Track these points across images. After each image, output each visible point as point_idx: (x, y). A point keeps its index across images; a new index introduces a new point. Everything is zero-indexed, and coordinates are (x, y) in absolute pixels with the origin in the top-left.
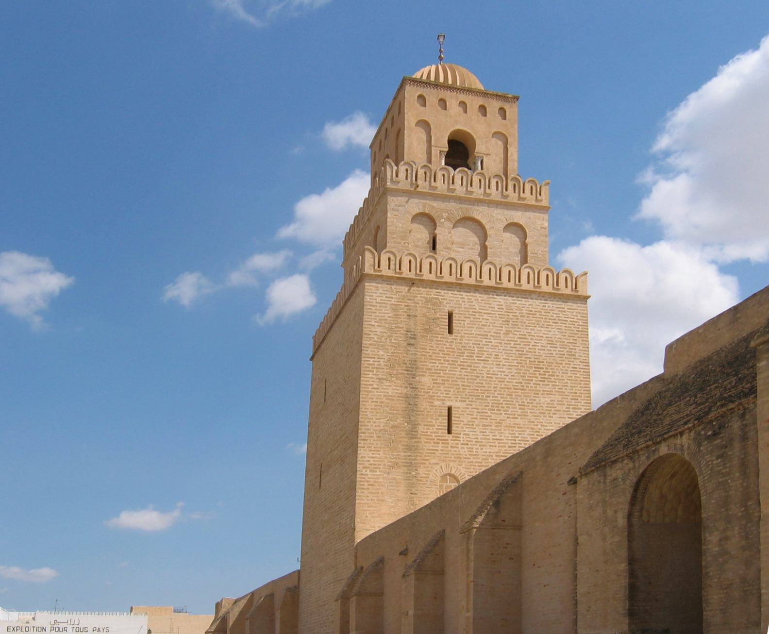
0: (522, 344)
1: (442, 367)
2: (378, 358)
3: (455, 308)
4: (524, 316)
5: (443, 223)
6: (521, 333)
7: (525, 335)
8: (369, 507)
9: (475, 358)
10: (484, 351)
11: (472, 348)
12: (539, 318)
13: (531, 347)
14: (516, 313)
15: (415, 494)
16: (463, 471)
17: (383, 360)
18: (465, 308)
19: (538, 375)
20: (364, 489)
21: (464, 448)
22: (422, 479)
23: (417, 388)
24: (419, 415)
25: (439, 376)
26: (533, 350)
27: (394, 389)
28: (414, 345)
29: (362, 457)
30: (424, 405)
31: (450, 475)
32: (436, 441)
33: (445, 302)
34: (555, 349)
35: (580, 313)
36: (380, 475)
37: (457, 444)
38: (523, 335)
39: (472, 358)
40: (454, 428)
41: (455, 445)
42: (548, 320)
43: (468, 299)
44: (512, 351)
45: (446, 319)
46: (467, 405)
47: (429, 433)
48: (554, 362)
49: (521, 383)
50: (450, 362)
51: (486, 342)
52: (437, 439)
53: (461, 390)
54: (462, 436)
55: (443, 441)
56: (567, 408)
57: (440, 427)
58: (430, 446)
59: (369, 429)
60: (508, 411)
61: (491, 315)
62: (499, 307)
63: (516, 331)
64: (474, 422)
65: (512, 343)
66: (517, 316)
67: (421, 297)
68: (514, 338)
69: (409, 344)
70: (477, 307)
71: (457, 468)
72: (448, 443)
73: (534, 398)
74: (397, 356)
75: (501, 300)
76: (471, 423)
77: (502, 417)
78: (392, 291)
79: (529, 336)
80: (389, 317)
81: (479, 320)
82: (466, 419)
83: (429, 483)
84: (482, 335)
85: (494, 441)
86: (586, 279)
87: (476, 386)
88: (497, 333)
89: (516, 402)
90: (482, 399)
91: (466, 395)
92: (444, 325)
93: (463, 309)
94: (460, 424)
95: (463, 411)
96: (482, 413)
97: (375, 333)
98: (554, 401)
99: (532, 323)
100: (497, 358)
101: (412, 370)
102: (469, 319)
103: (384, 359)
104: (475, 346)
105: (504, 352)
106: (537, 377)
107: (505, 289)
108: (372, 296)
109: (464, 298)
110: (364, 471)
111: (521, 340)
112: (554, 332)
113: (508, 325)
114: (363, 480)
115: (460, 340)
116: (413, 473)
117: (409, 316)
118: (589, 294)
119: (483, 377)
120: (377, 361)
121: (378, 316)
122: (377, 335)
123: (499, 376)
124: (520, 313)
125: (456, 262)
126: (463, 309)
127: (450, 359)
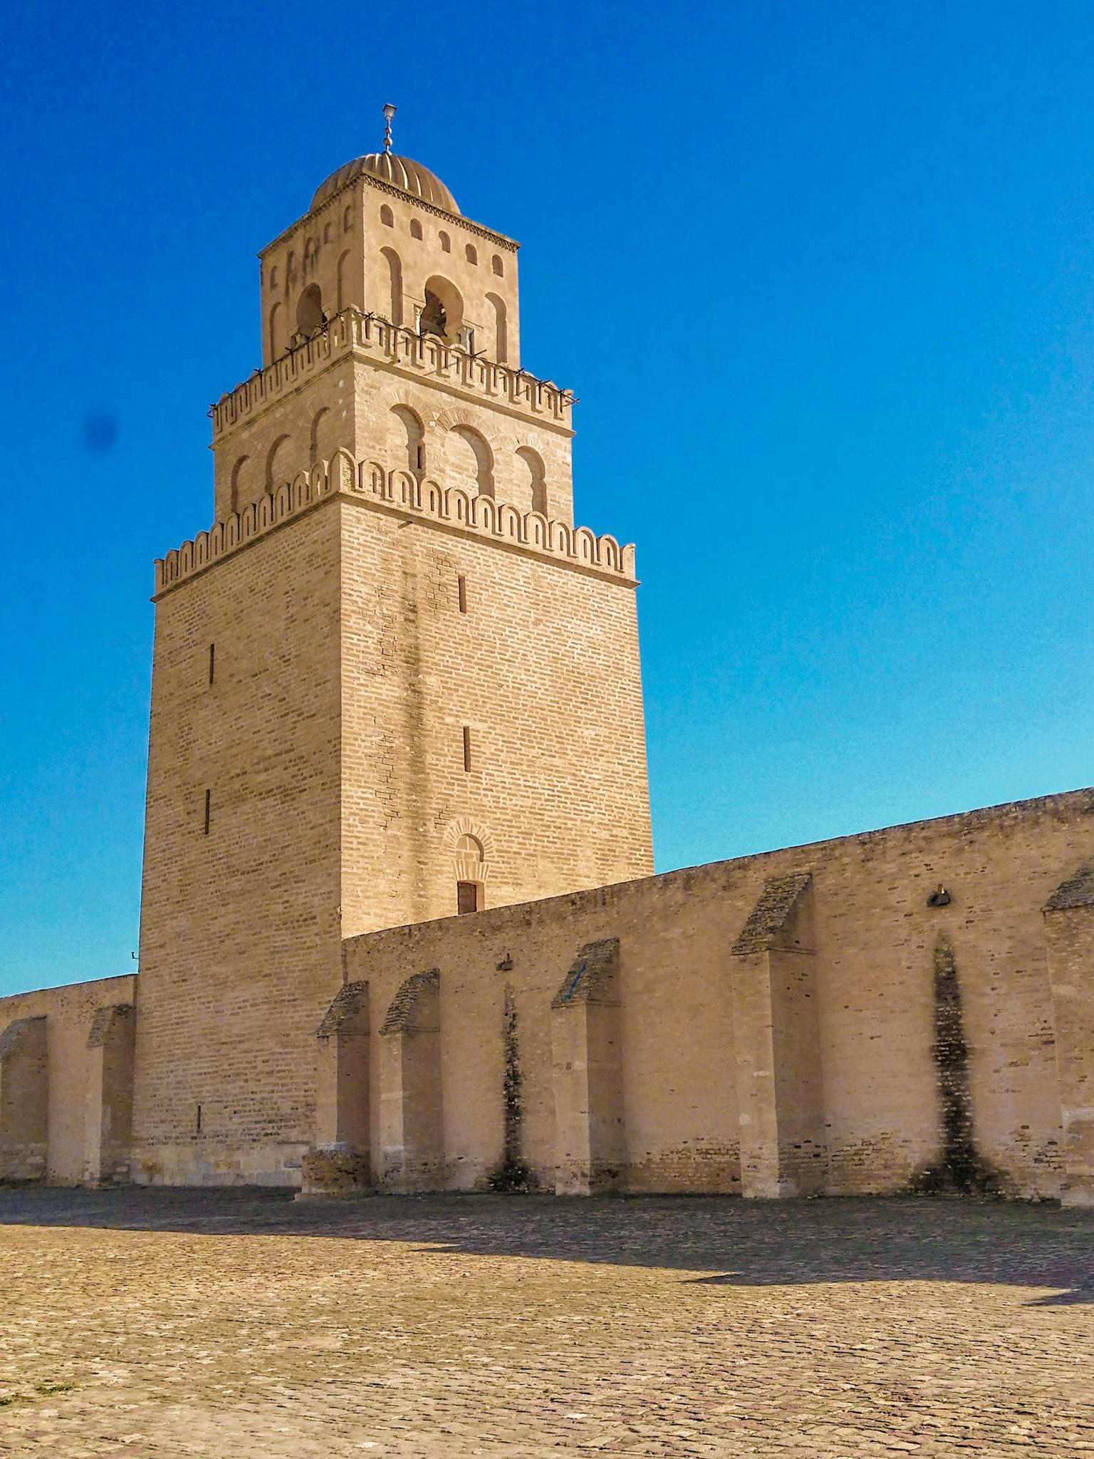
8: (361, 880)
15: (425, 863)
16: (488, 832)
21: (486, 795)
23: (420, 692)
27: (390, 689)
29: (348, 797)
30: (430, 719)
31: (470, 836)
37: (478, 788)
54: (483, 776)
70: (496, 574)
75: (528, 565)
101: (414, 661)
117: (405, 573)
125: (466, 498)
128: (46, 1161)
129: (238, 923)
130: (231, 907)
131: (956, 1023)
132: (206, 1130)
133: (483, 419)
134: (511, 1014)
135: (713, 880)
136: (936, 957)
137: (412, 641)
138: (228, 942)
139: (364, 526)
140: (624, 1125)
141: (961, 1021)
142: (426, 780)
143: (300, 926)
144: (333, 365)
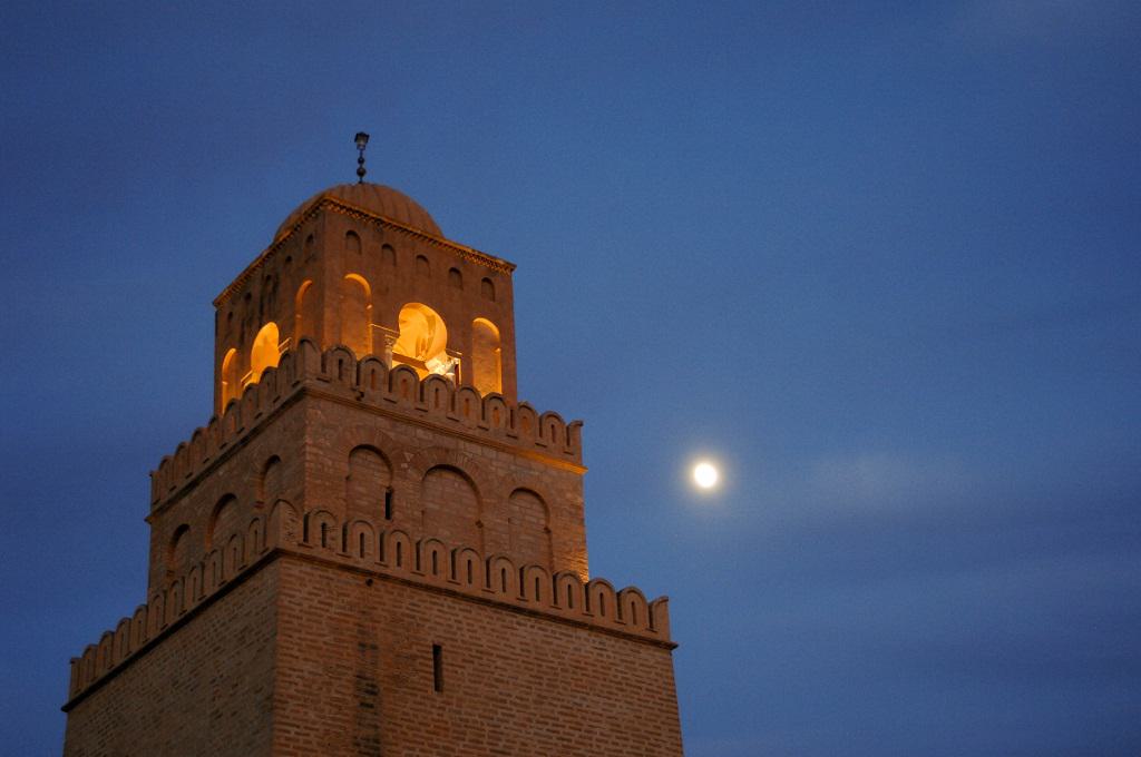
0: (568, 725)
2: (306, 728)
3: (446, 639)
4: (566, 671)
5: (405, 470)
6: (565, 703)
9: (485, 746)
10: (502, 733)
11: (479, 726)
12: (594, 677)
13: (583, 733)
14: (552, 662)
17: (315, 732)
18: (463, 641)
26: (586, 741)
28: (372, 706)
33: (428, 625)
34: (625, 742)
38: (567, 708)
39: (480, 745)
42: (607, 683)
43: (468, 624)
44: (551, 738)
51: (503, 714)
61: (510, 662)
62: (524, 647)
63: (554, 699)
65: (550, 721)
67: (383, 610)
68: (553, 711)
69: (362, 704)
70: (483, 642)
74: (341, 727)
75: (527, 630)
78: (331, 592)
80: (325, 643)
81: (487, 669)
84: (496, 700)
86: (666, 610)
88: (522, 699)
92: (427, 672)
93: (459, 643)
97: (300, 674)
99: (582, 687)
100: (525, 751)
102: (471, 665)
103: (317, 730)
105: (536, 738)
107: (533, 613)
109: (460, 622)
111: (567, 718)
112: (621, 707)
113: (540, 684)
117: (361, 645)
118: (673, 640)
120: (304, 735)
121: (305, 639)
122: (302, 678)
124: (559, 663)
126: (459, 643)
127: (441, 744)
133: (467, 454)
137: (371, 732)
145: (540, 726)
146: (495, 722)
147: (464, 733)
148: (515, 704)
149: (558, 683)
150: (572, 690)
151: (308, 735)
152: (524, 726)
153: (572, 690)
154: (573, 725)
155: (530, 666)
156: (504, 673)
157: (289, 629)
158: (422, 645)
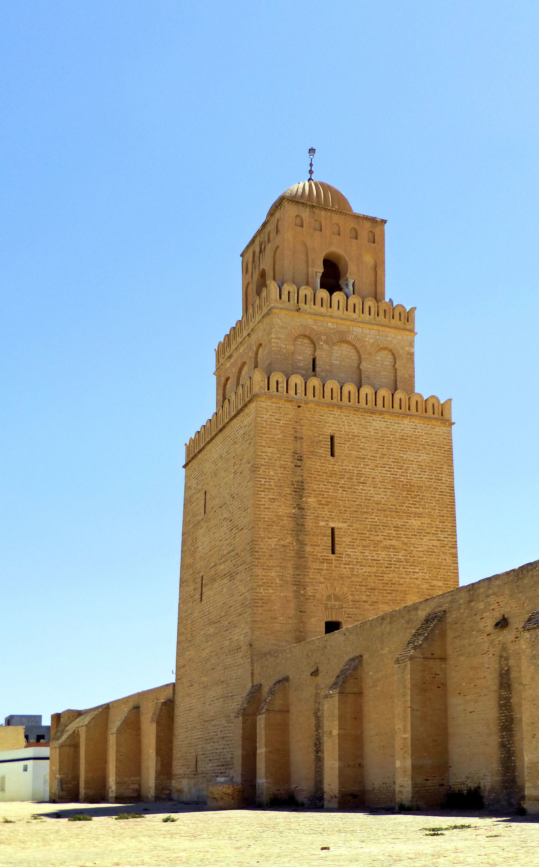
0: (396, 467)
1: (325, 488)
6: (394, 457)
7: (398, 459)
10: (363, 474)
19: (410, 499)
20: (258, 607)
21: (346, 568)
22: (310, 597)
24: (306, 535)
25: (323, 498)
26: (405, 474)
30: (309, 523)
32: (321, 560)
34: (424, 473)
35: (445, 439)
36: (273, 593)
38: (396, 459)
40: (337, 548)
41: (338, 565)
42: (417, 445)
44: (387, 474)
45: (328, 442)
46: (349, 526)
47: (315, 553)
48: (423, 485)
49: (395, 505)
50: (333, 484)
52: (323, 559)
53: (343, 511)
55: (328, 561)
56: (435, 531)
57: (325, 547)
58: (317, 565)
59: (261, 548)
60: (384, 532)
63: (390, 455)
64: (354, 542)
66: (391, 440)
71: (341, 587)
72: (332, 563)
73: (407, 521)
76: (352, 544)
77: (378, 538)
79: (402, 460)
82: (347, 540)
83: (316, 601)
85: (372, 561)
87: (356, 508)
89: (391, 524)
90: (361, 521)
91: (347, 516)
94: (342, 544)
95: (345, 532)
96: (362, 534)
98: (425, 523)
104: (355, 469)
106: (409, 500)
108: (263, 418)
110: (258, 589)
111: (396, 464)
112: (424, 456)
114: (257, 598)
115: (341, 463)
116: (302, 592)
119: (362, 499)
123: (376, 499)
128: (140, 785)
129: (212, 652)
130: (209, 643)
131: (509, 702)
132: (199, 770)
134: (318, 702)
135: (403, 617)
136: (500, 661)
138: (208, 663)
139: (269, 413)
140: (363, 767)
141: (512, 701)
142: (306, 561)
143: (235, 653)
144: (263, 317)
145: (382, 469)
146: (360, 469)
147: (345, 475)
148: (370, 459)
149: (392, 448)
150: (399, 450)
151: (270, 482)
152: (374, 470)
153: (399, 450)
154: (399, 467)
155: (379, 440)
156: (365, 445)
157: (260, 433)
158: (325, 435)
